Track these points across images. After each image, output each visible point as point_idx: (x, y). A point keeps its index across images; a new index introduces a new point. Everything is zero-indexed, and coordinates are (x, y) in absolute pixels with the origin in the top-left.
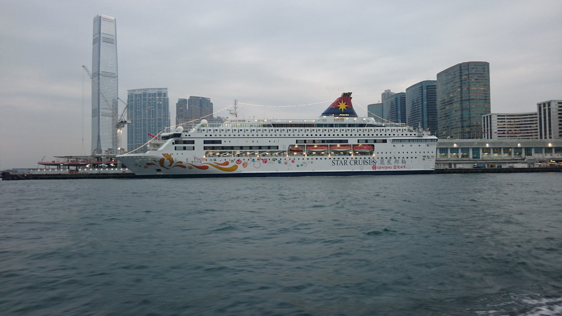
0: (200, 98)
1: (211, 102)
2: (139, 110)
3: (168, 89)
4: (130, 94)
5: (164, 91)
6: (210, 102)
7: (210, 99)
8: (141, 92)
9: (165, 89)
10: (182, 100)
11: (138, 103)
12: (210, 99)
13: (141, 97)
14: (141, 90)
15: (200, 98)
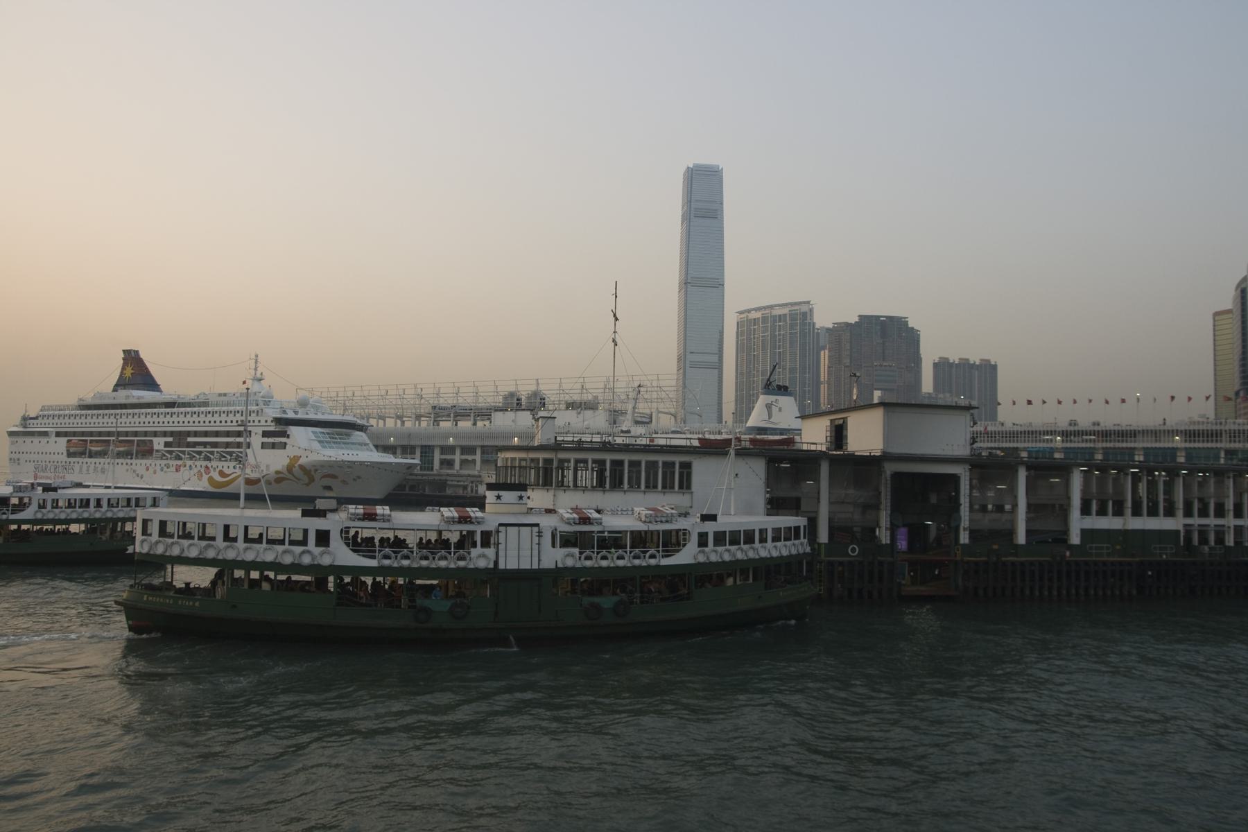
0: (882, 319)
1: (910, 326)
2: (781, 350)
3: (811, 303)
4: (739, 320)
5: (804, 308)
6: (907, 324)
7: (906, 320)
8: (785, 311)
9: (804, 303)
10: (843, 325)
11: (754, 338)
12: (906, 320)
13: (785, 321)
14: (786, 305)
15: (882, 319)
